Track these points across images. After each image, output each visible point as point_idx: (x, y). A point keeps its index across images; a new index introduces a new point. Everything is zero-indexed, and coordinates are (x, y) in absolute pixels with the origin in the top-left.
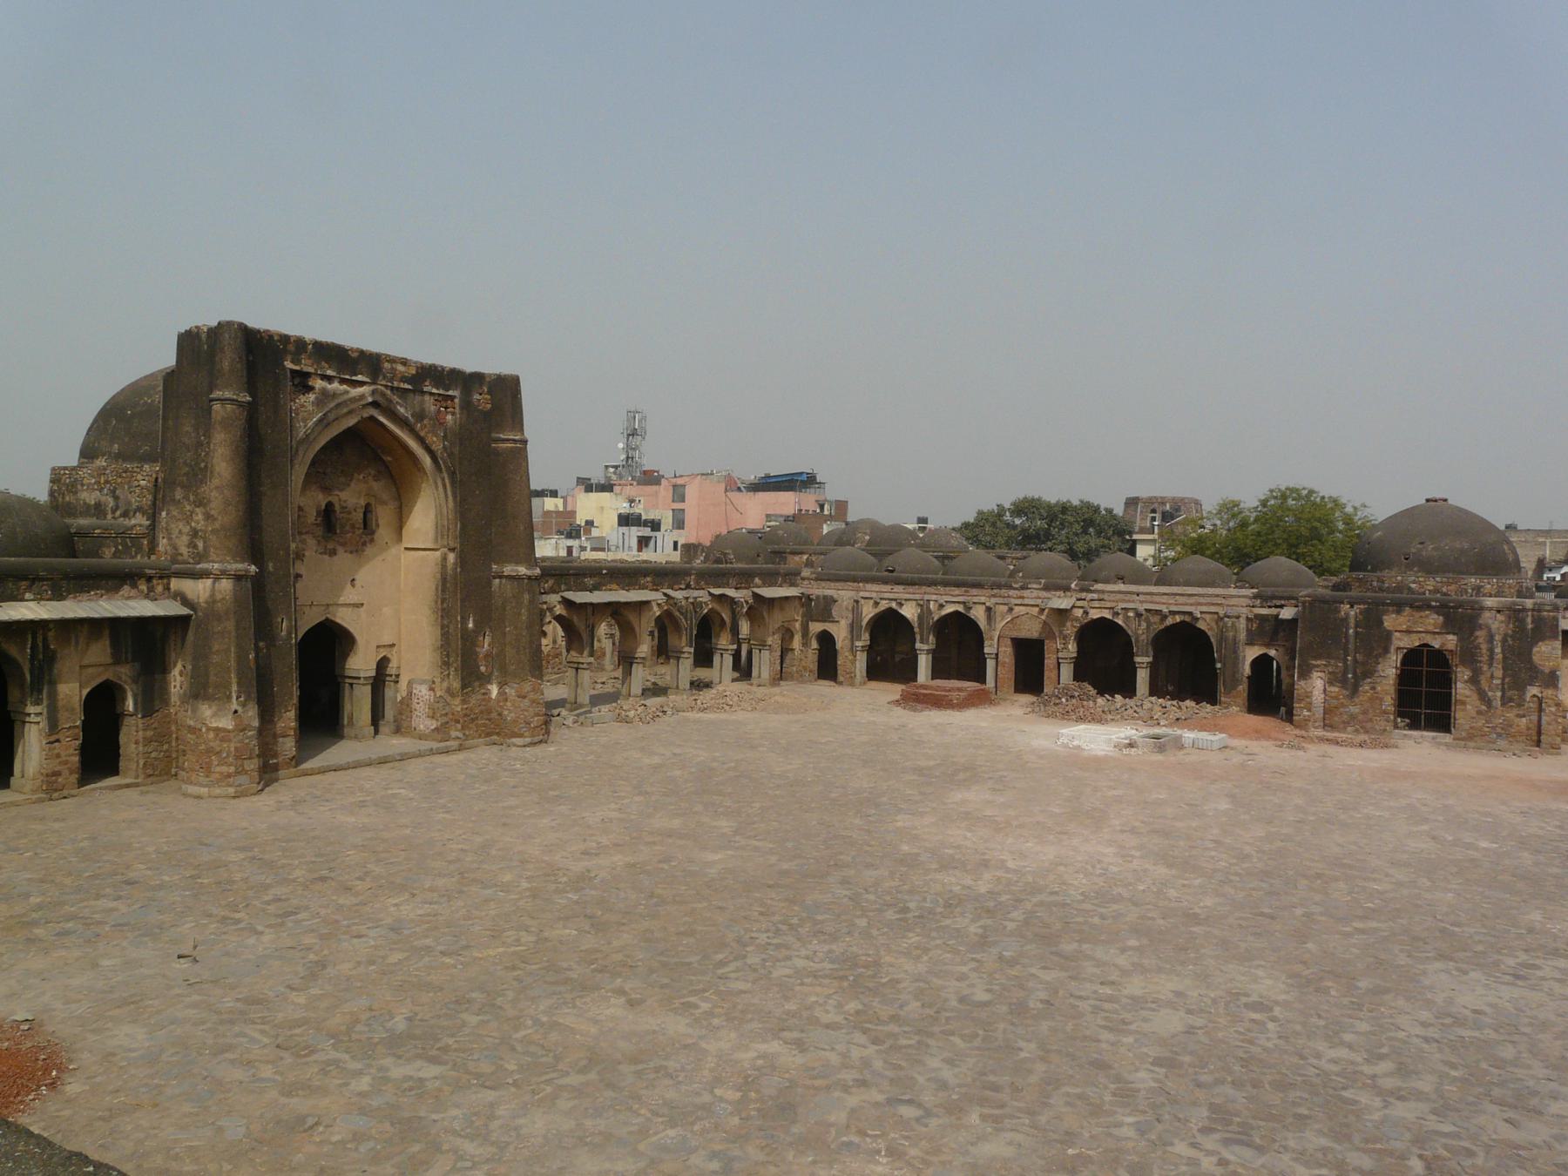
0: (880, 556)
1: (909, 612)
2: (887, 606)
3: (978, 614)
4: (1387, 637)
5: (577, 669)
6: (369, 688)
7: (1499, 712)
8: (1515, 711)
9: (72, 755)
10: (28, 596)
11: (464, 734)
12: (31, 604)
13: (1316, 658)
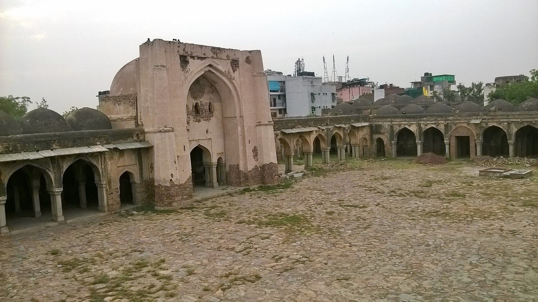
0: (399, 108)
1: (413, 128)
2: (404, 127)
3: (442, 128)
5: (288, 157)
6: (216, 168)
9: (118, 198)
10: (98, 143)
11: (250, 184)
12: (100, 146)
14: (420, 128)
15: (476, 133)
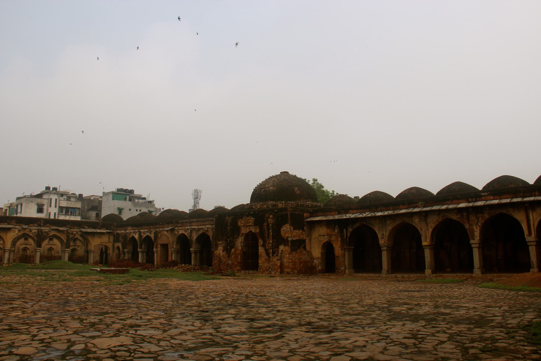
1: (137, 236)
3: (152, 236)
8: (277, 258)
13: (219, 241)
14: (140, 236)
15: (172, 240)
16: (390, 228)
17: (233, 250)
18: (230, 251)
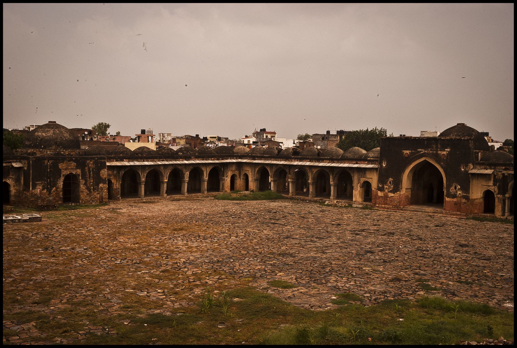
4: (59, 171)
7: (92, 193)
8: (97, 193)
16: (147, 171)
17: (54, 188)
18: (51, 189)
